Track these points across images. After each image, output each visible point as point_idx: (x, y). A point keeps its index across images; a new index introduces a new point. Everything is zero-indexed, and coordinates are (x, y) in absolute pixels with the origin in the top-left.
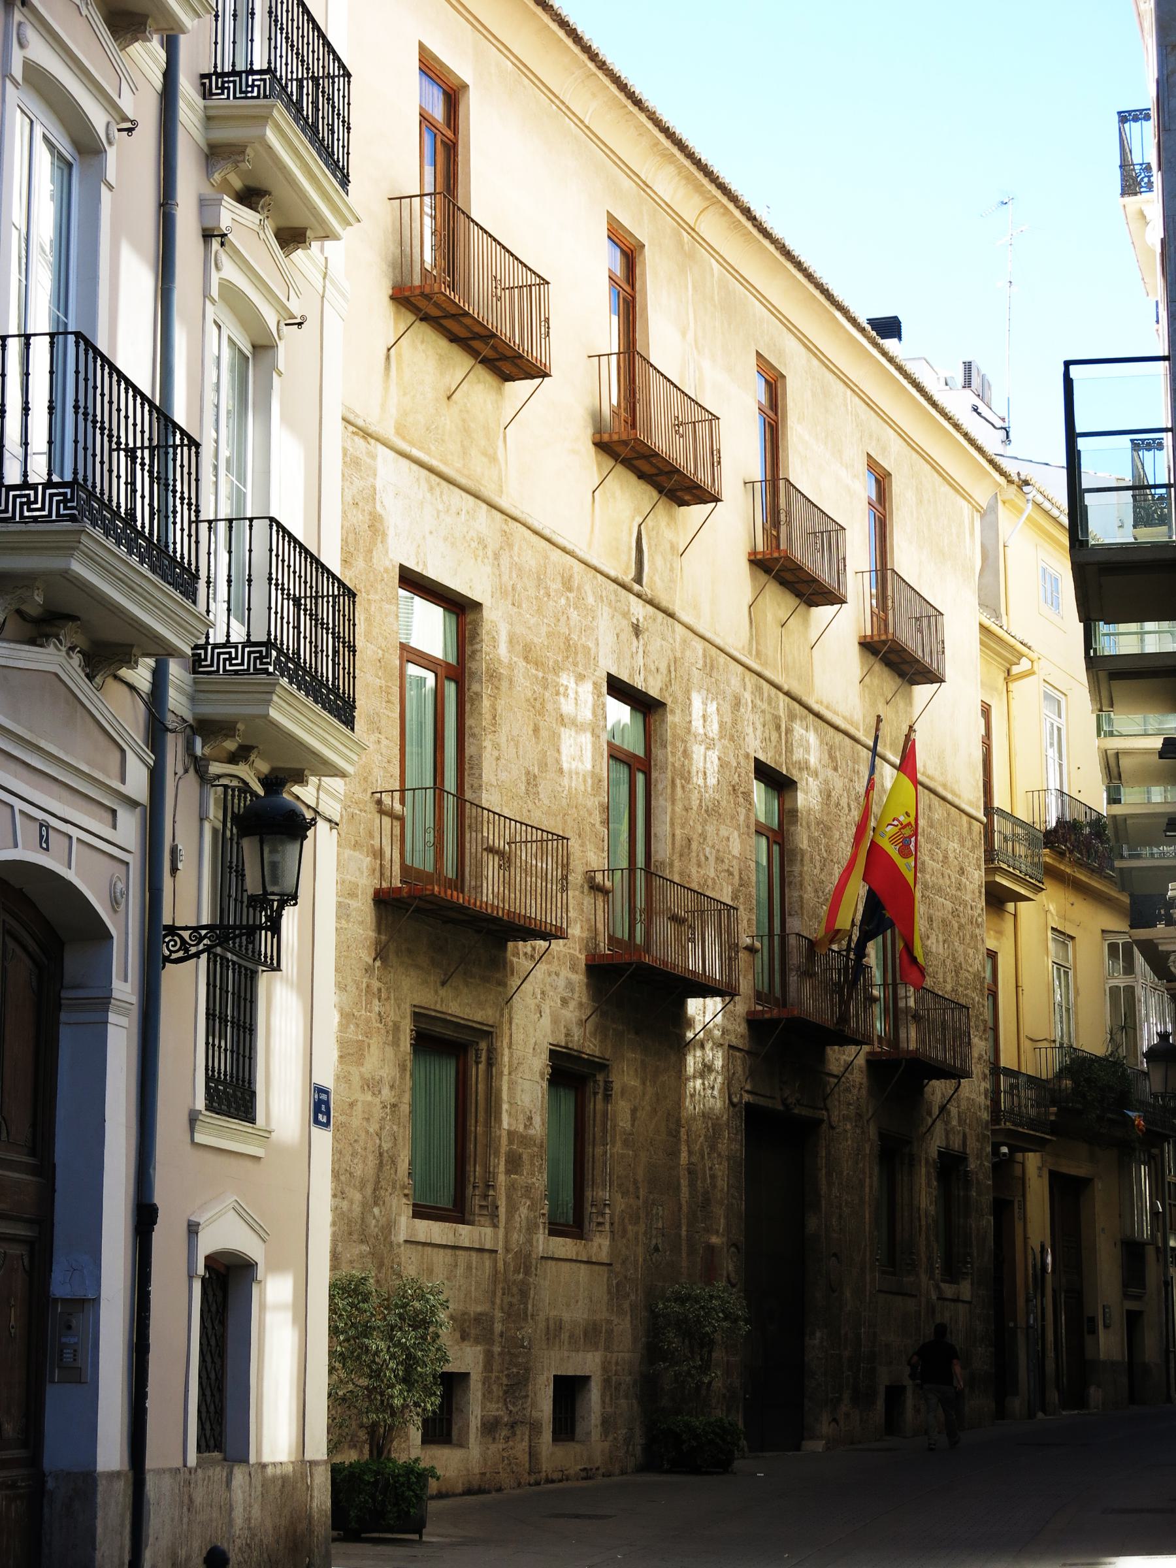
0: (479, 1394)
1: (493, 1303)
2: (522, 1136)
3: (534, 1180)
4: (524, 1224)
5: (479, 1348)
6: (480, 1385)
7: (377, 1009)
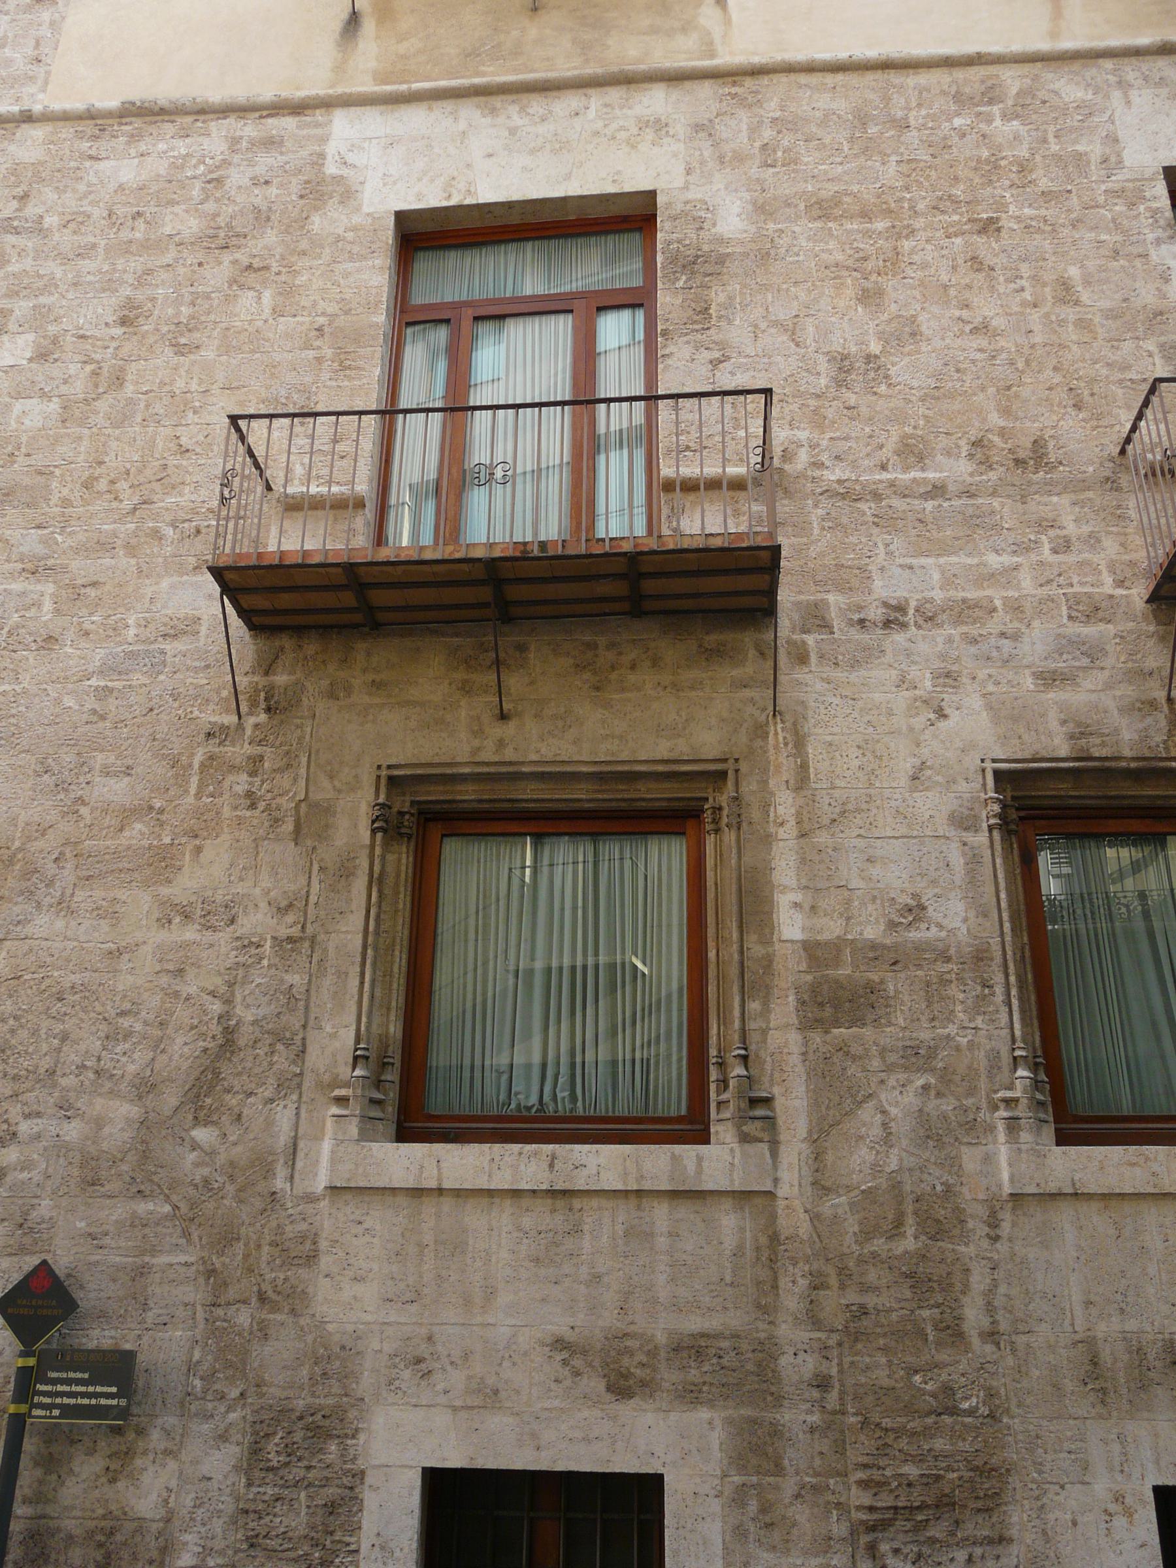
0: (715, 1531)
1: (766, 1309)
2: (873, 946)
3: (952, 1029)
4: (903, 1127)
5: (704, 1414)
6: (715, 1506)
7: (240, 789)
